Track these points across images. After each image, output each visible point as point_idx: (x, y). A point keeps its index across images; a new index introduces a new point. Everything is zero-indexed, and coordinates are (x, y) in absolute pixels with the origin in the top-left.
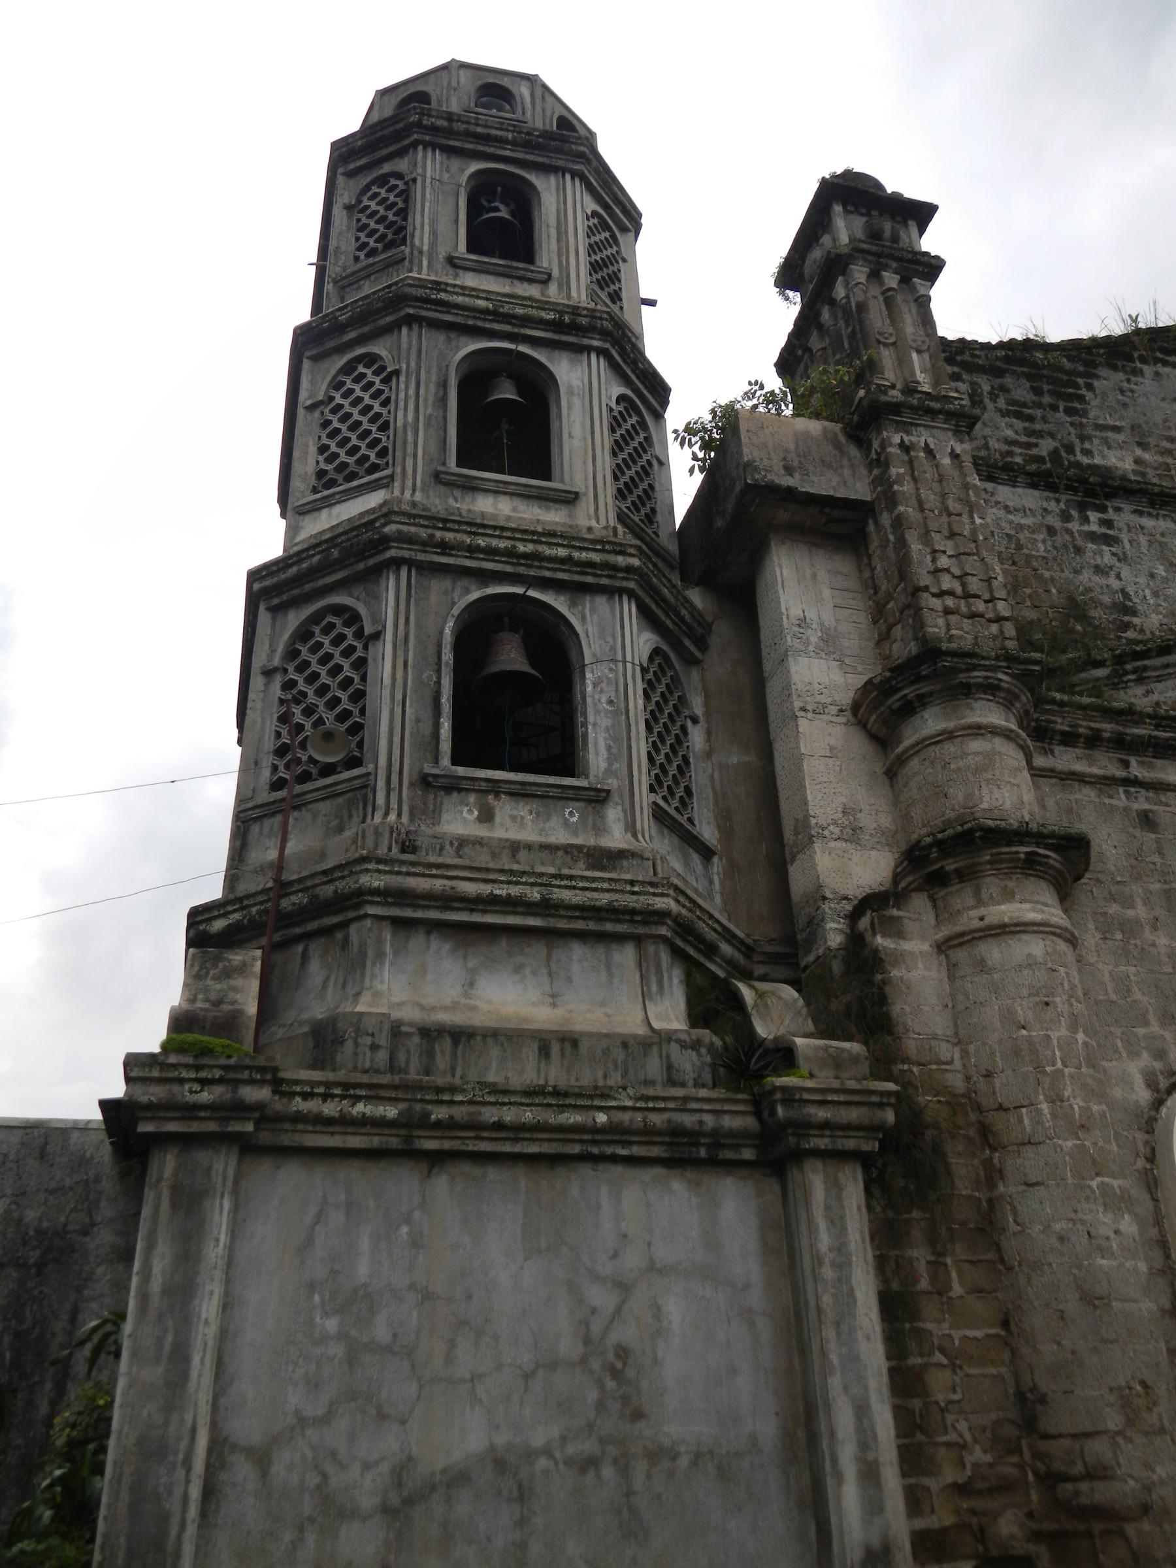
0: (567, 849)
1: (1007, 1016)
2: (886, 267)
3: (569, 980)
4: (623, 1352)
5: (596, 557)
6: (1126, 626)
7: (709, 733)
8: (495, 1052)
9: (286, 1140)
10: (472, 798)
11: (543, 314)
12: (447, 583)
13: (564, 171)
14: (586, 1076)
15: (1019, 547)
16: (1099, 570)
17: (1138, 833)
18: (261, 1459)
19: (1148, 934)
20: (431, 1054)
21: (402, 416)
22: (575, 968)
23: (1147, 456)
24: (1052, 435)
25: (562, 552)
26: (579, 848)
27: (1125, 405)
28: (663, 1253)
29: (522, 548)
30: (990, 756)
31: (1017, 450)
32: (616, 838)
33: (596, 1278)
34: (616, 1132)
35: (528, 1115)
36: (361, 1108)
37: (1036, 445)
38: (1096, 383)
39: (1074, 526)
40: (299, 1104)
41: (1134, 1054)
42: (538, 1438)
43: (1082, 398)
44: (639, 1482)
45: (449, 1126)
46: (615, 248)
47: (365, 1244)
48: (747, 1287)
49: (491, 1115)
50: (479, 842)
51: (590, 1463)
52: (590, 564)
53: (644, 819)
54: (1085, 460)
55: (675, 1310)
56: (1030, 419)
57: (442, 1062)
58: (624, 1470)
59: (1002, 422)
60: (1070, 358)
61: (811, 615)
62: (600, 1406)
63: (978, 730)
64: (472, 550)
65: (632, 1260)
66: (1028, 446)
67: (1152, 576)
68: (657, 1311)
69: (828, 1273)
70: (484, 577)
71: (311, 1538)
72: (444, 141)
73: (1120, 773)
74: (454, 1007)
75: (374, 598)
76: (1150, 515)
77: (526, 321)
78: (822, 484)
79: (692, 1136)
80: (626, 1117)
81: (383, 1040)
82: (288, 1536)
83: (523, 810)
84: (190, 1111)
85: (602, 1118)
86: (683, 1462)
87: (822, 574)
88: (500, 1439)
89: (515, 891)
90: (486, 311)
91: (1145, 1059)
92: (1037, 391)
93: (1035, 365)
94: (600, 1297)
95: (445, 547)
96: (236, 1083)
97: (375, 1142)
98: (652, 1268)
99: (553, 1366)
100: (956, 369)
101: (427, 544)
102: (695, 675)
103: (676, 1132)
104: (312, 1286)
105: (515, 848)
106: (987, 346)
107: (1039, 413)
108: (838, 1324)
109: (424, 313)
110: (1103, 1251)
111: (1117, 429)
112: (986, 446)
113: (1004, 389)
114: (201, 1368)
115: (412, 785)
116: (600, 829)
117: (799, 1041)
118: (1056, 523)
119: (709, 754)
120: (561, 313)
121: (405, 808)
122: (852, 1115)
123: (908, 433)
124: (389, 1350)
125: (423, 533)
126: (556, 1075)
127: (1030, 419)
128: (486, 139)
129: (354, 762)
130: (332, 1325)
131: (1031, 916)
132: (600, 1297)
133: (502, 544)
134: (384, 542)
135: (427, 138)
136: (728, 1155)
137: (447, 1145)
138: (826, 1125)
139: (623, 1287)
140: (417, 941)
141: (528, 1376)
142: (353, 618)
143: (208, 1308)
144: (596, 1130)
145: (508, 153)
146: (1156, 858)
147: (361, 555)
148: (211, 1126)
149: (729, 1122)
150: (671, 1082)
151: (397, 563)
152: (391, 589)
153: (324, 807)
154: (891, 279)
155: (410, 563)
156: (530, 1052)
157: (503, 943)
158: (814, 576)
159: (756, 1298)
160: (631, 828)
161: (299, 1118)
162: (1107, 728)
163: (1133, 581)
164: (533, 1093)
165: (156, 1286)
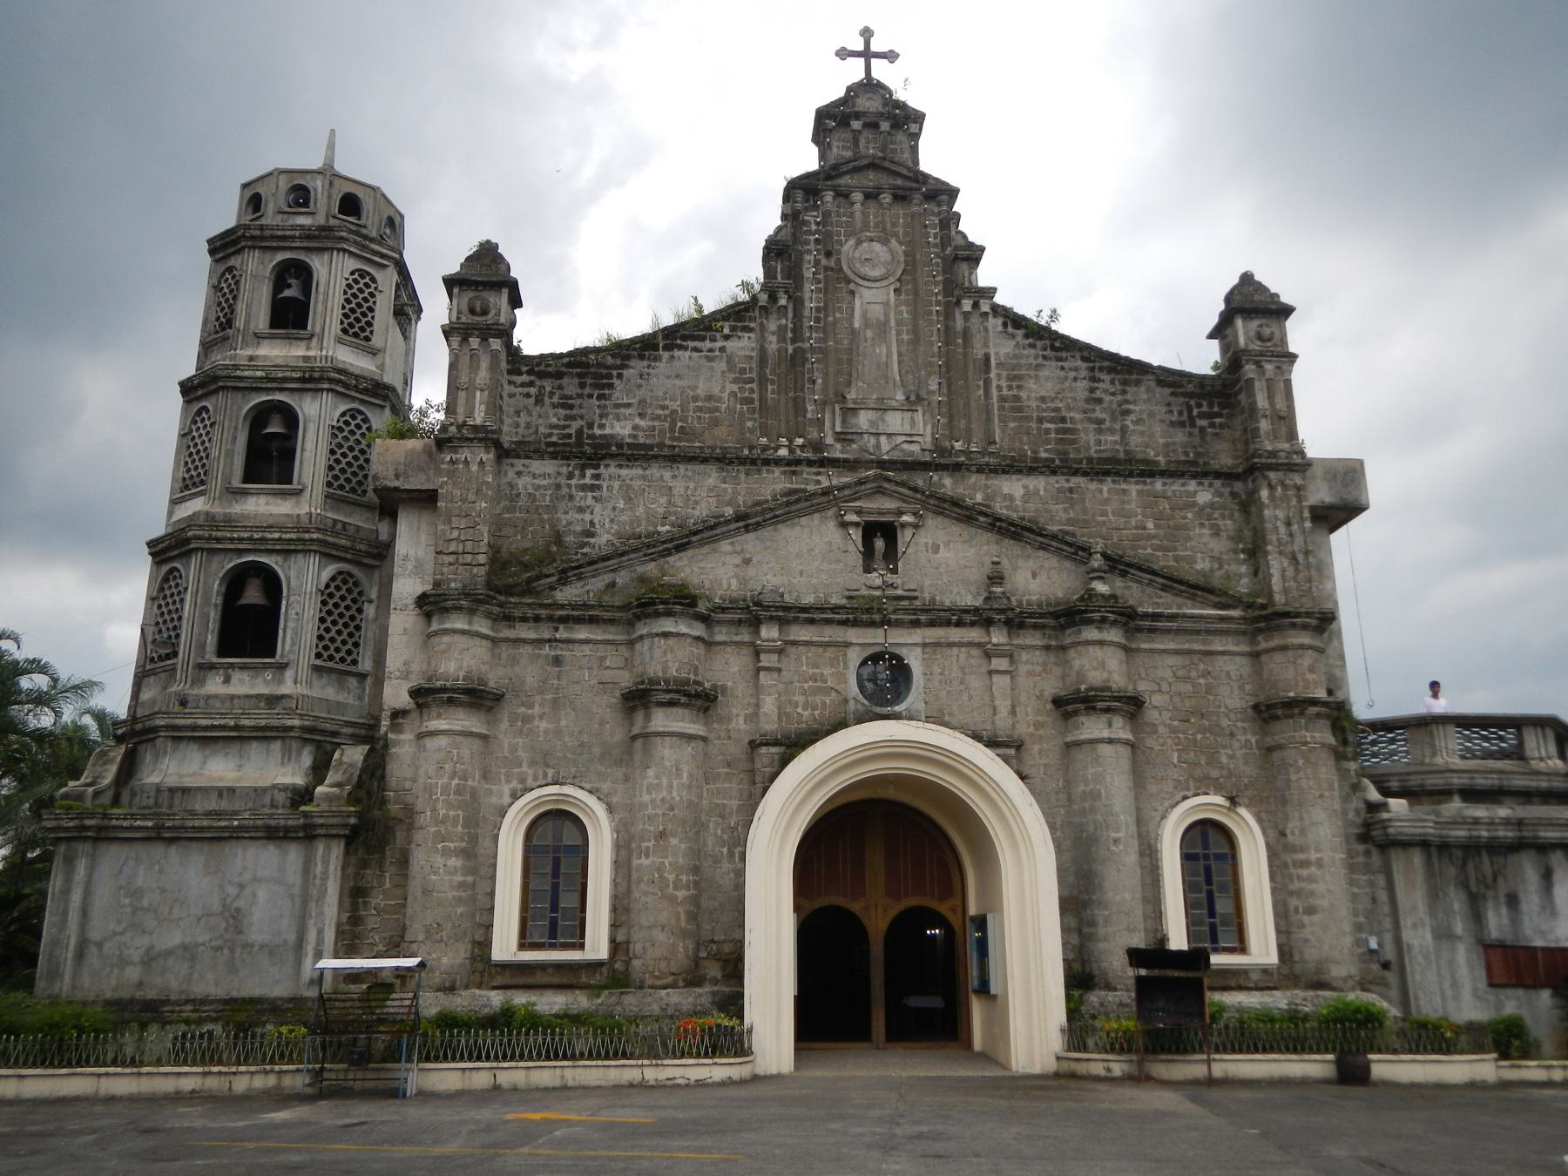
0: (259, 697)
1: (426, 772)
2: (471, 335)
3: (249, 758)
4: (238, 910)
5: (293, 536)
7: (378, 607)
8: (199, 796)
9: (111, 835)
10: (221, 671)
11: (294, 375)
12: (222, 557)
13: (332, 249)
14: (237, 805)
15: (534, 500)
16: (581, 510)
17: (549, 668)
18: (100, 945)
19: (536, 722)
20: (172, 798)
21: (214, 453)
22: (253, 752)
23: (642, 423)
24: (582, 417)
25: (276, 535)
26: (262, 695)
27: (641, 386)
28: (260, 873)
29: (256, 536)
30: (449, 645)
31: (555, 432)
32: (287, 688)
33: (231, 882)
34: (241, 828)
35: (205, 823)
36: (138, 823)
37: (569, 426)
38: (625, 372)
39: (573, 482)
40: (114, 822)
41: (508, 781)
43: (611, 386)
44: (237, 955)
45: (173, 828)
46: (373, 286)
47: (142, 873)
48: (294, 886)
49: (190, 823)
50: (216, 696)
51: (220, 948)
52: (291, 540)
54: (597, 432)
55: (262, 894)
56: (571, 407)
57: (177, 802)
58: (232, 950)
59: (551, 412)
60: (613, 356)
61: (412, 552)
62: (226, 929)
63: (446, 632)
64: (232, 540)
65: (247, 876)
66: (565, 427)
67: (614, 509)
68: (254, 895)
69: (318, 882)
70: (240, 552)
71: (116, 971)
72: (259, 244)
73: (547, 636)
74: (194, 774)
76: (628, 466)
77: (285, 380)
78: (416, 483)
79: (277, 828)
80: (246, 822)
81: (152, 794)
82: (108, 970)
83: (245, 676)
84: (67, 829)
85: (236, 823)
86: (256, 948)
87: (424, 527)
88: (187, 940)
89: (223, 722)
90: (262, 378)
91: (515, 784)
92: (582, 386)
93: (587, 366)
94: (232, 891)
95: (218, 540)
96: (82, 819)
97: (145, 835)
98: (255, 879)
99: (210, 915)
100: (532, 378)
101: (210, 539)
102: (376, 574)
103: (268, 828)
104: (121, 888)
105: (232, 697)
106: (561, 356)
107: (577, 402)
108: (317, 901)
109: (229, 384)
110: (435, 873)
111: (628, 405)
112: (536, 432)
113: (560, 388)
115: (194, 668)
116: (281, 682)
118: (563, 481)
119: (376, 620)
120: (304, 372)
121: (189, 680)
122: (334, 821)
123: (456, 453)
124: (147, 910)
125: (207, 534)
126: (224, 805)
127: (571, 407)
128: (284, 238)
130: (127, 901)
131: (446, 727)
132: (232, 891)
133: (246, 535)
134: (188, 541)
135: (250, 243)
136: (293, 835)
137: (174, 835)
138: (322, 825)
139: (241, 887)
140: (183, 745)
141: (199, 919)
144: (233, 827)
145: (298, 244)
146: (556, 682)
148: (76, 834)
149: (290, 823)
150: (272, 806)
152: (194, 562)
153: (163, 675)
154: (474, 342)
155: (202, 549)
156: (214, 796)
157: (221, 743)
158: (419, 528)
159: (297, 890)
161: (115, 827)
162: (544, 613)
163: (600, 514)
164: (208, 814)
165: (57, 890)
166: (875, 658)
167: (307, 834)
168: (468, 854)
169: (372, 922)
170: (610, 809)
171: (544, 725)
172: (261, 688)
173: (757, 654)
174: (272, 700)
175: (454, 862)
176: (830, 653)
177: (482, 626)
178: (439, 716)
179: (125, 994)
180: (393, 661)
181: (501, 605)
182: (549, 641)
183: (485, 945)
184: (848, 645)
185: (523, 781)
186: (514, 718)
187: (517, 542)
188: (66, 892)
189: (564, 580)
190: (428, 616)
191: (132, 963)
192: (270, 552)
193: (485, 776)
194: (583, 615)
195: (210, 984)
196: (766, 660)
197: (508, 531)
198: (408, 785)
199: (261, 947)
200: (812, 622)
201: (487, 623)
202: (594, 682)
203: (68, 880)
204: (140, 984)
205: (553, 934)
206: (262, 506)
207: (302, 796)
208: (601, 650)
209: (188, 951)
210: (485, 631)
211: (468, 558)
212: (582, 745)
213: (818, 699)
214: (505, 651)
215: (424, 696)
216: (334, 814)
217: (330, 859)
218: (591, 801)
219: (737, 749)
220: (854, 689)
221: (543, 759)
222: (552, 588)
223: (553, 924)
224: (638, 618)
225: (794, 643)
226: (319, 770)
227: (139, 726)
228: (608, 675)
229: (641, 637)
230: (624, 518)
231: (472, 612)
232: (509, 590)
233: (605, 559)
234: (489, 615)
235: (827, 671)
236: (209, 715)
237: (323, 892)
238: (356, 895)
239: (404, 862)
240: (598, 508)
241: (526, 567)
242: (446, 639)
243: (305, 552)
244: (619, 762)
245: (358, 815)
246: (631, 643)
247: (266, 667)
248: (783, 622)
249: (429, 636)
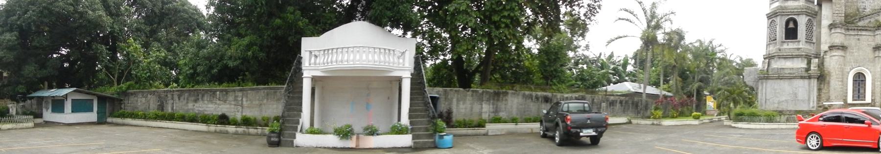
4: (796, 93)
6: (864, 11)
14: (794, 72)
34: (796, 76)
55: (800, 90)
63: (836, 33)
67: (870, 2)
68: (799, 90)
73: (856, 34)
94: (795, 89)
99: (790, 94)
103: (801, 76)
114: (764, 95)
126: (791, 72)
139: (796, 88)
143: (764, 90)
156: (789, 70)
162: (856, 28)
164: (789, 73)
167: (810, 78)
168: (842, 81)
169: (823, 95)
170: (871, 73)
171: (856, 54)
175: (840, 83)
177: (843, 31)
178: (836, 52)
179: (775, 109)
180: (823, 40)
181: (847, 26)
182: (857, 35)
183: (845, 101)
185: (852, 66)
186: (850, 52)
187: (850, 11)
188: (762, 89)
189: (860, 21)
190: (831, 29)
191: (775, 103)
193: (844, 65)
194: (864, 29)
195: (792, 108)
197: (847, 8)
198: (829, 67)
199: (801, 100)
201: (844, 30)
202: (867, 44)
203: (762, 87)
204: (778, 108)
205: (859, 98)
207: (808, 69)
208: (868, 37)
210: (844, 33)
211: (840, 15)
212: (864, 58)
214: (848, 37)
215: (832, 48)
216: (815, 73)
217: (814, 82)
218: (867, 70)
221: (856, 61)
222: (857, 22)
223: (859, 96)
224: (876, 30)
226: (809, 63)
228: (869, 43)
229: (877, 34)
230: (872, 5)
231: (841, 28)
232: (849, 23)
233: (869, 15)
234: (845, 29)
237: (814, 89)
238: (819, 90)
239: (829, 83)
240: (866, 2)
241: (852, 17)
242: (836, 34)
244: (872, 62)
245: (820, 73)
246: (874, 36)
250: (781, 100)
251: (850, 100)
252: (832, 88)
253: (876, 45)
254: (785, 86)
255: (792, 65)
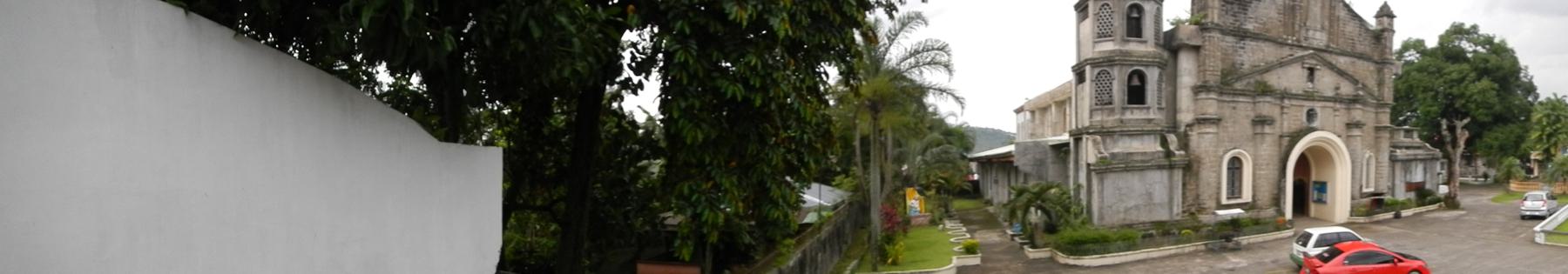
0: (1145, 119)
21: (1116, 24)
32: (1152, 116)
34: (1151, 166)
42: (1140, 203)
51: (1145, 206)
53: (1156, 111)
55: (1157, 187)
70: (1132, 65)
75: (1112, 70)
94: (1148, 186)
105: (1137, 120)
116: (1148, 113)
117: (1177, 152)
129: (1111, 103)
134: (1115, 61)
140: (1124, 138)
142: (1108, 73)
147: (1110, 61)
151: (1116, 65)
160: (1154, 113)
166: (1311, 110)
167: (1171, 167)
172: (1143, 117)
173: (1282, 108)
174: (1150, 121)
176: (1299, 108)
184: (1303, 106)
192: (1142, 65)
196: (1285, 110)
200: (1297, 99)
206: (1134, 47)
209: (1137, 207)
213: (1297, 122)
217: (1178, 175)
219: (1276, 137)
220: (1304, 118)
225: (1292, 105)
227: (1105, 130)
235: (1299, 114)
236: (1133, 127)
243: (1153, 66)
247: (1144, 108)
248: (1290, 98)
249: (1197, 100)
250: (1129, 206)
251: (1224, 201)
252: (1203, 183)
253: (1257, 117)
254: (1134, 182)
255: (1141, 147)
